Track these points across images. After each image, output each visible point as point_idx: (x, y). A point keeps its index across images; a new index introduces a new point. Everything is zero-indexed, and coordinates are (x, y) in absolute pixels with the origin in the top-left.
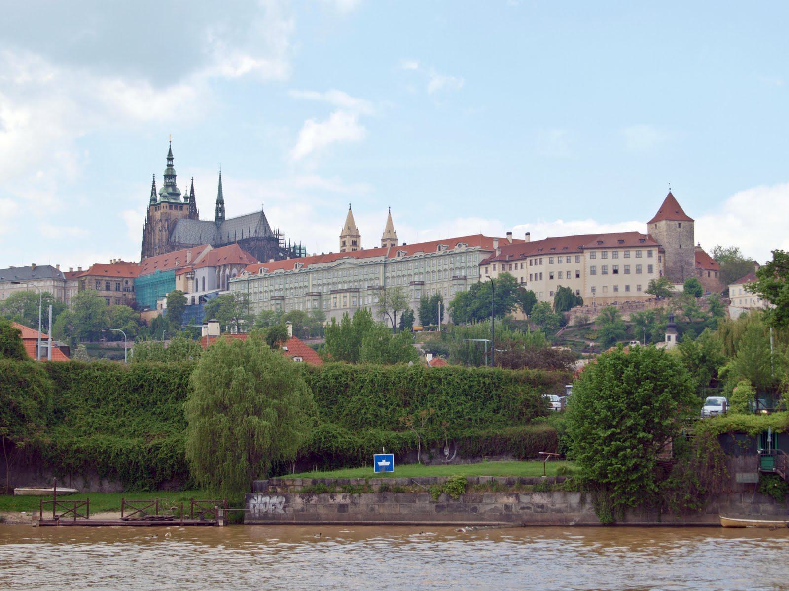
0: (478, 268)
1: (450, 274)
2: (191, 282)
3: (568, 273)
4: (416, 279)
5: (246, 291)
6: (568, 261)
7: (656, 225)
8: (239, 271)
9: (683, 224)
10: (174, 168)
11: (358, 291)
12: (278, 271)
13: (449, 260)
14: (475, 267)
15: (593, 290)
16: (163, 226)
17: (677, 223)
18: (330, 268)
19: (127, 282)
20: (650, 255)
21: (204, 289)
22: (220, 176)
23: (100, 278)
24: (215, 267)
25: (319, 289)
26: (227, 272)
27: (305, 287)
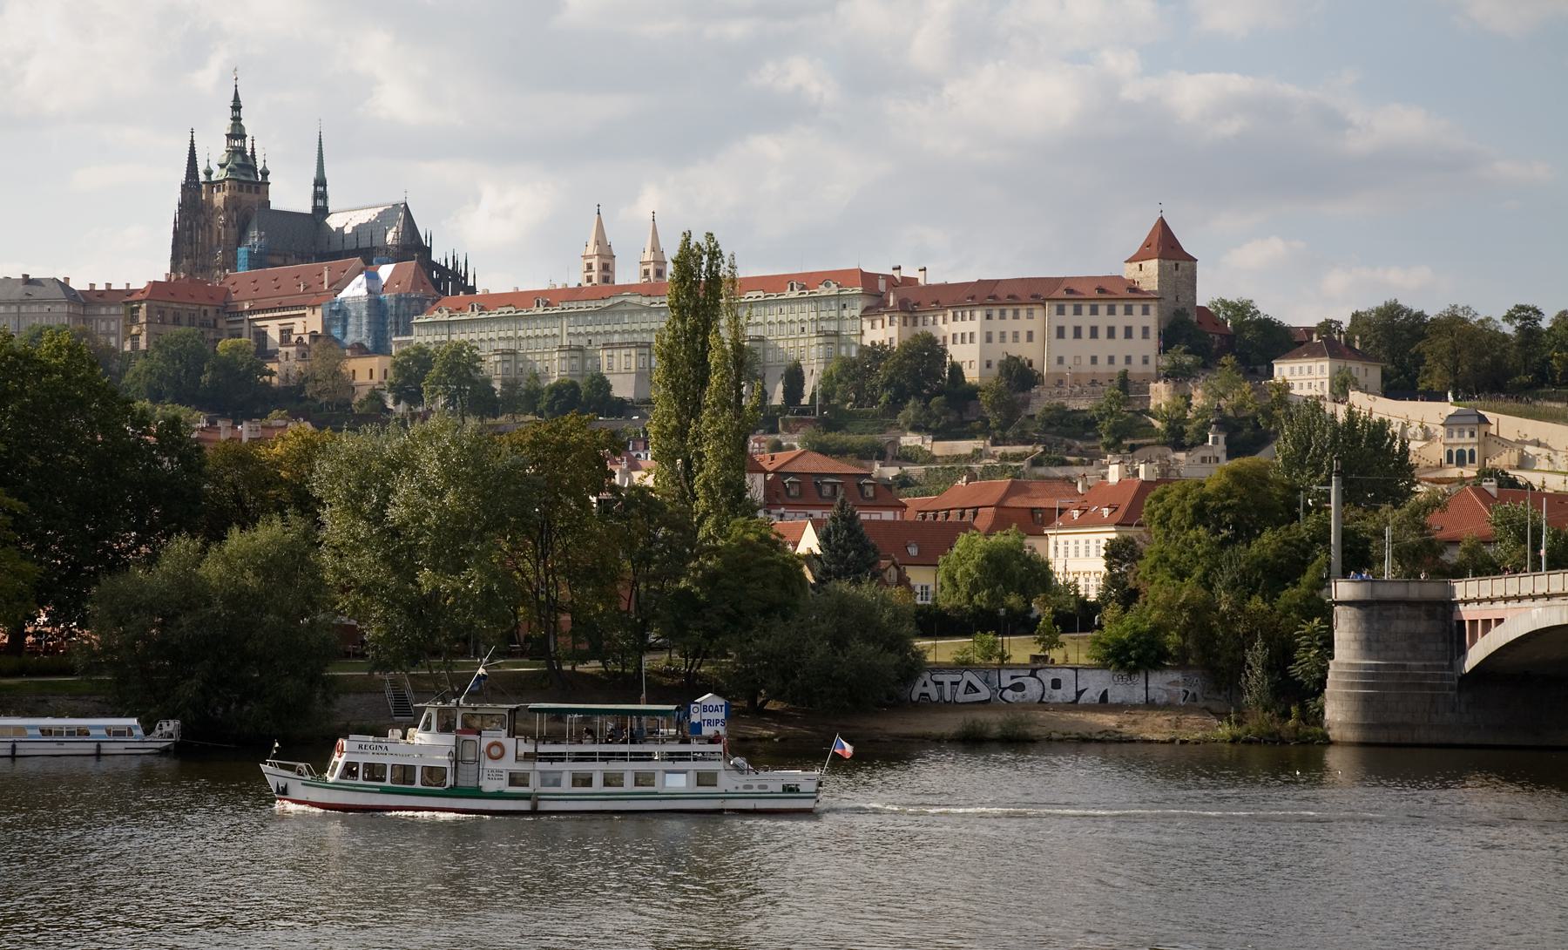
1: (809, 327)
3: (1016, 335)
6: (1016, 316)
7: (1141, 265)
9: (1181, 264)
10: (242, 122)
12: (506, 310)
13: (807, 307)
14: (853, 318)
15: (1060, 360)
17: (1173, 263)
19: (205, 311)
20: (1146, 311)
21: (359, 333)
22: (320, 142)
23: (164, 304)
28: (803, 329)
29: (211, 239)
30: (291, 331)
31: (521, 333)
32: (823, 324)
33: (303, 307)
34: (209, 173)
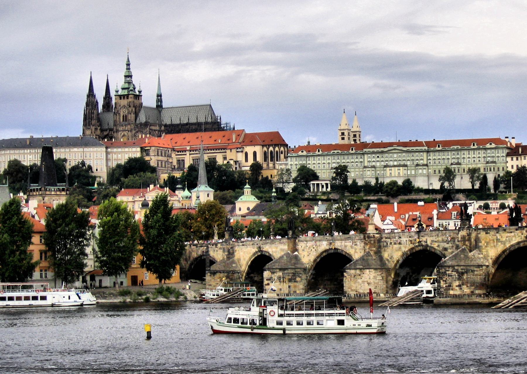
0: (504, 158)
1: (482, 160)
2: (240, 154)
4: (453, 161)
5: (304, 162)
8: (284, 149)
11: (406, 166)
12: (336, 151)
13: (482, 152)
14: (503, 156)
16: (132, 110)
18: (382, 152)
22: (159, 77)
23: (158, 148)
24: (263, 146)
25: (374, 164)
26: (277, 149)
27: (361, 162)
28: (474, 161)
29: (119, 118)
30: (215, 158)
31: (343, 161)
32: (489, 158)
33: (224, 149)
34: (117, 91)
